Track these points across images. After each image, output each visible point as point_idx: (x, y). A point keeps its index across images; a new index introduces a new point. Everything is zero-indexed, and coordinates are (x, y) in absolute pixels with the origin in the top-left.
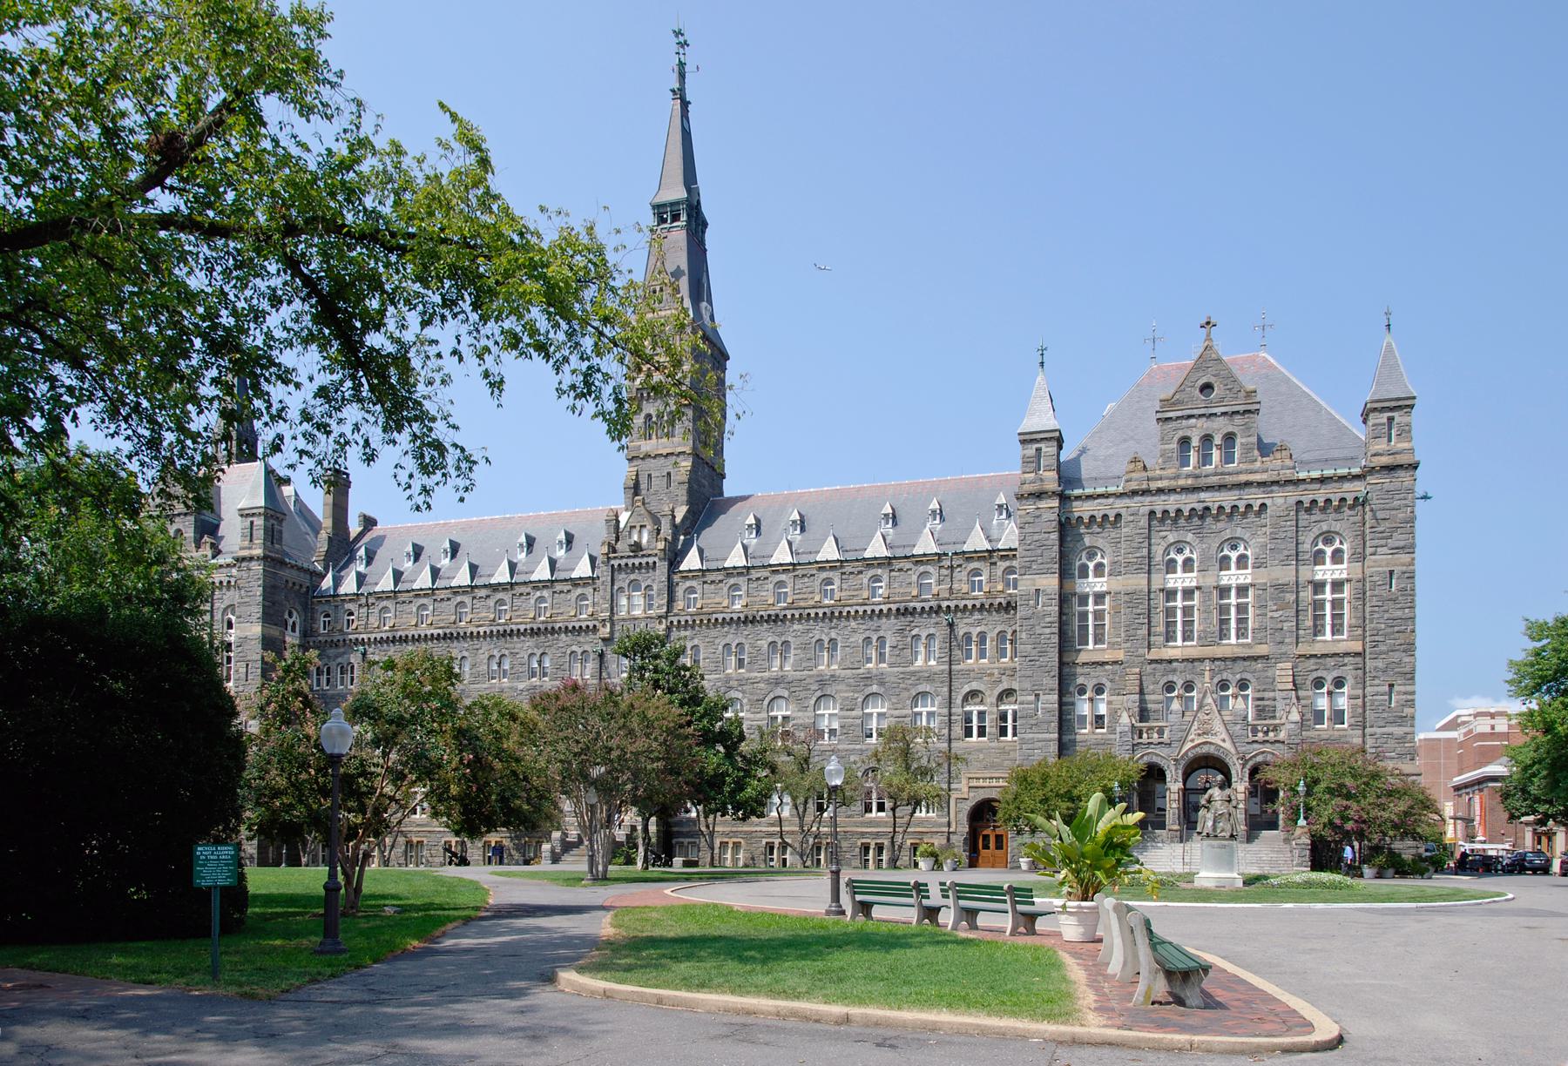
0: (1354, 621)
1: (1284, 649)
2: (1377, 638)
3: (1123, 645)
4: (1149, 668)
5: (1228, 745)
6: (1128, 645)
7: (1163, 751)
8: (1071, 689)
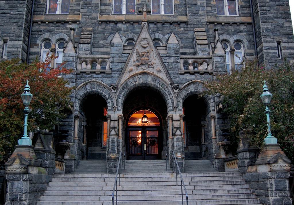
0: (243, 3)
1: (199, 18)
2: (265, 8)
3: (82, 10)
4: (100, 28)
5: (163, 75)
6: (85, 10)
7: (106, 81)
8: (39, 42)
